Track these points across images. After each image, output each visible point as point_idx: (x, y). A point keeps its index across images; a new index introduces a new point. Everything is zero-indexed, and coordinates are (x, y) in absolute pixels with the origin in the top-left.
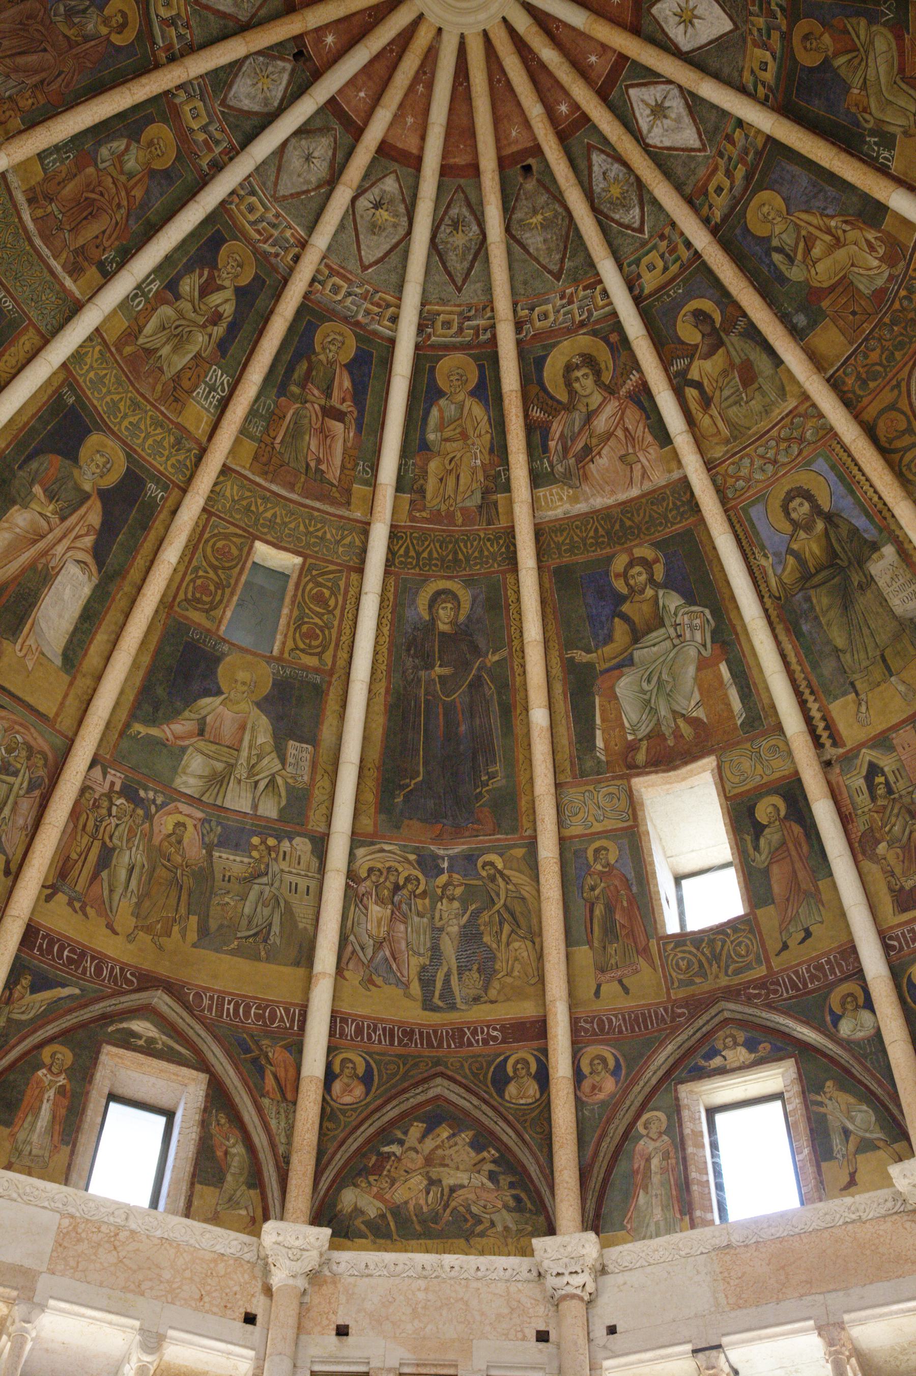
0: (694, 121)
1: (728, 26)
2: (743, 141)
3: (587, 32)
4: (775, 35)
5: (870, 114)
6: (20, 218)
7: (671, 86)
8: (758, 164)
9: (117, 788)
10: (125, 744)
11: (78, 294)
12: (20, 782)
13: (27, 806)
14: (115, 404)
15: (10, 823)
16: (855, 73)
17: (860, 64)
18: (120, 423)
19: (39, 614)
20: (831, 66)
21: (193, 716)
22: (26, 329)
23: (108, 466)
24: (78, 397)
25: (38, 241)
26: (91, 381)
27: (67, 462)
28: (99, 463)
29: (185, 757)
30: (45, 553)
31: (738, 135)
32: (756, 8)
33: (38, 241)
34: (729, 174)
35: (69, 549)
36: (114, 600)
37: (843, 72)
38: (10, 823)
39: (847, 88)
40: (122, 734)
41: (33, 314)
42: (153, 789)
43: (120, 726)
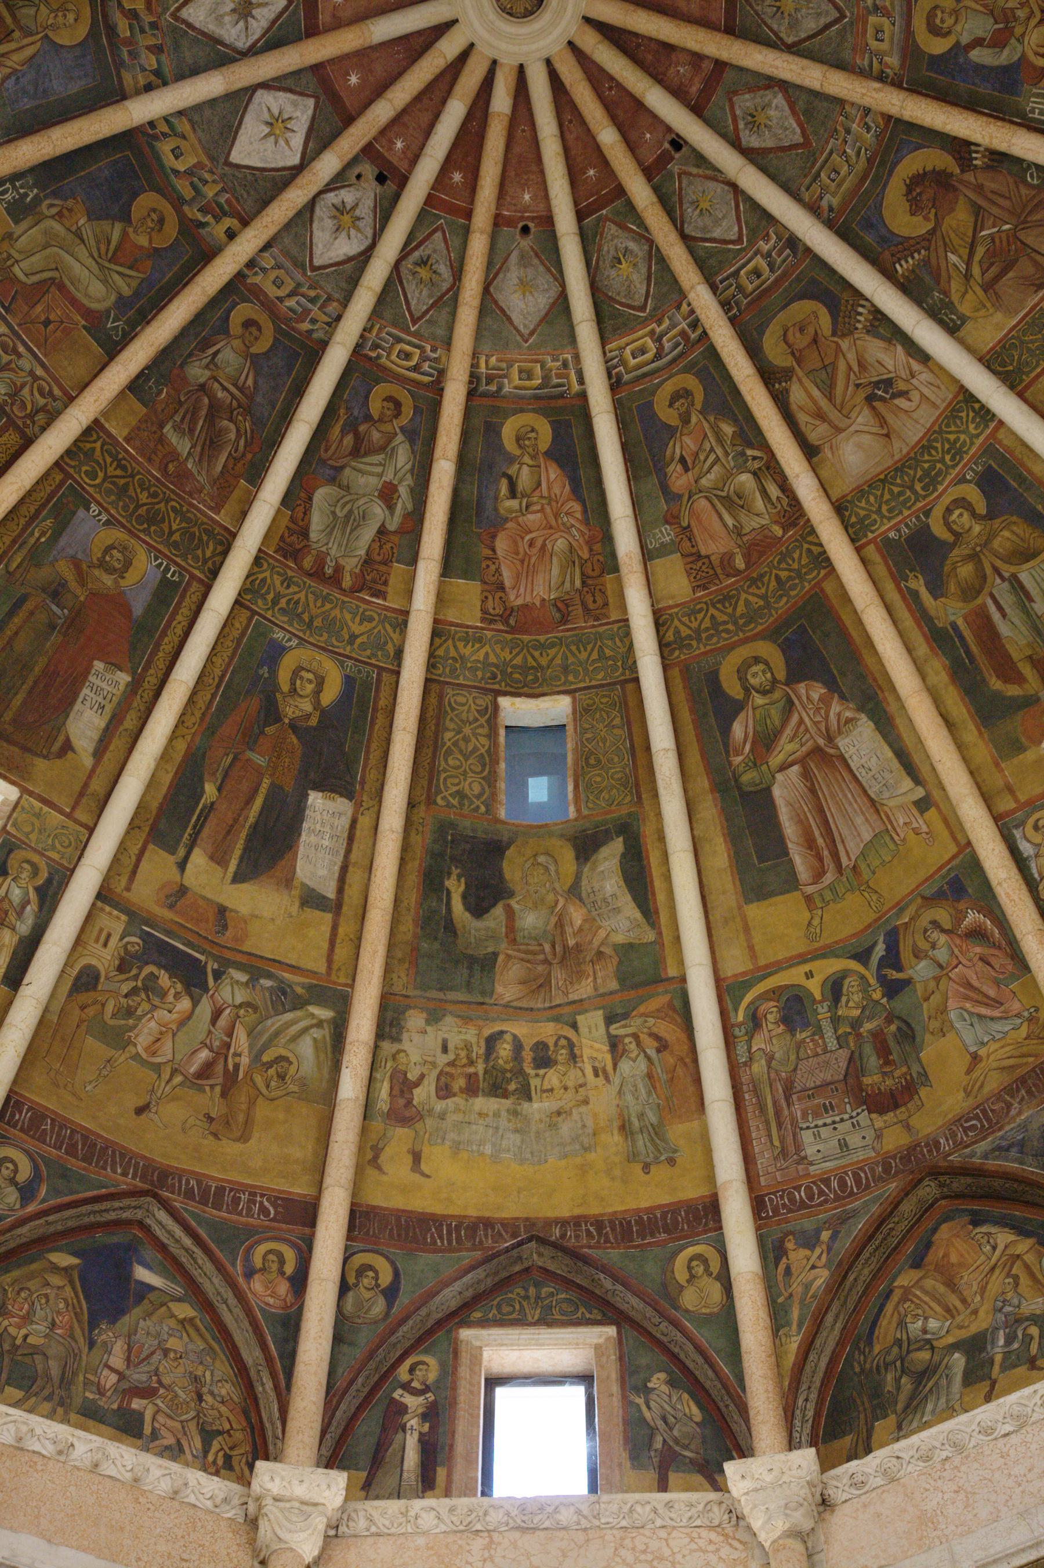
0: (203, 34)
1: (235, 157)
2: (142, 62)
3: (363, 25)
4: (188, 193)
5: (52, 217)
7: (248, 44)
8: (113, 54)
16: (95, 236)
17: (99, 250)
20: (121, 219)
31: (151, 61)
32: (222, 201)
34: (133, 15)
37: (106, 225)
39: (93, 216)
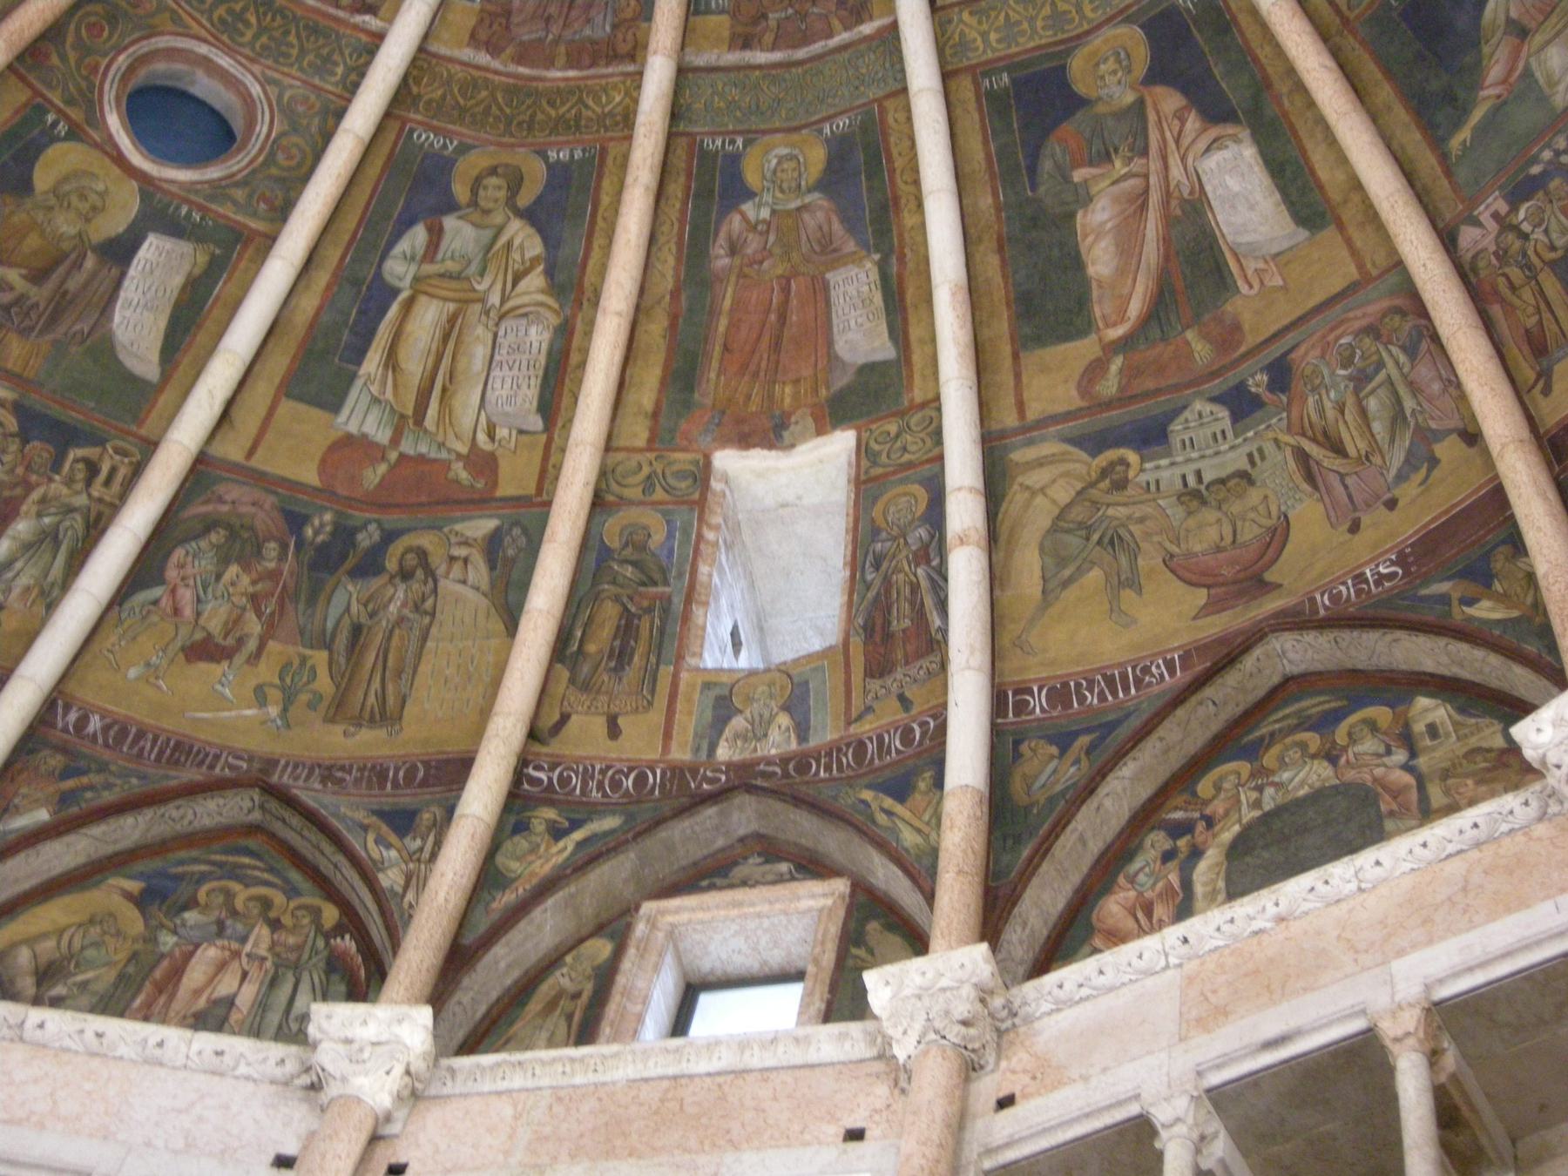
6: (760, 67)
9: (1502, 207)
10: (1462, 174)
11: (886, 21)
12: (1394, 360)
13: (1424, 372)
14: (1057, 19)
15: (1425, 405)
18: (1083, 17)
19: (1230, 238)
21: (1494, 41)
22: (882, 110)
23: (1123, 55)
24: (1009, 69)
25: (801, 54)
26: (999, 41)
27: (1079, 115)
28: (1110, 68)
29: (1538, 75)
30: (1168, 194)
33: (801, 54)
35: (1183, 159)
36: (1285, 115)
38: (1425, 405)
40: (1448, 173)
41: (873, 93)
42: (1541, 150)
43: (1439, 170)
